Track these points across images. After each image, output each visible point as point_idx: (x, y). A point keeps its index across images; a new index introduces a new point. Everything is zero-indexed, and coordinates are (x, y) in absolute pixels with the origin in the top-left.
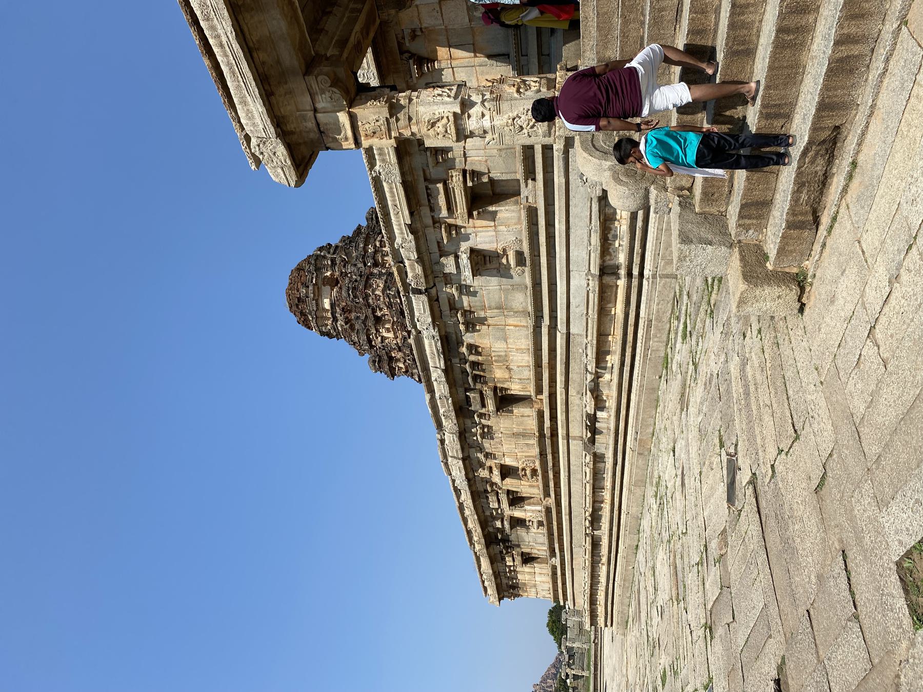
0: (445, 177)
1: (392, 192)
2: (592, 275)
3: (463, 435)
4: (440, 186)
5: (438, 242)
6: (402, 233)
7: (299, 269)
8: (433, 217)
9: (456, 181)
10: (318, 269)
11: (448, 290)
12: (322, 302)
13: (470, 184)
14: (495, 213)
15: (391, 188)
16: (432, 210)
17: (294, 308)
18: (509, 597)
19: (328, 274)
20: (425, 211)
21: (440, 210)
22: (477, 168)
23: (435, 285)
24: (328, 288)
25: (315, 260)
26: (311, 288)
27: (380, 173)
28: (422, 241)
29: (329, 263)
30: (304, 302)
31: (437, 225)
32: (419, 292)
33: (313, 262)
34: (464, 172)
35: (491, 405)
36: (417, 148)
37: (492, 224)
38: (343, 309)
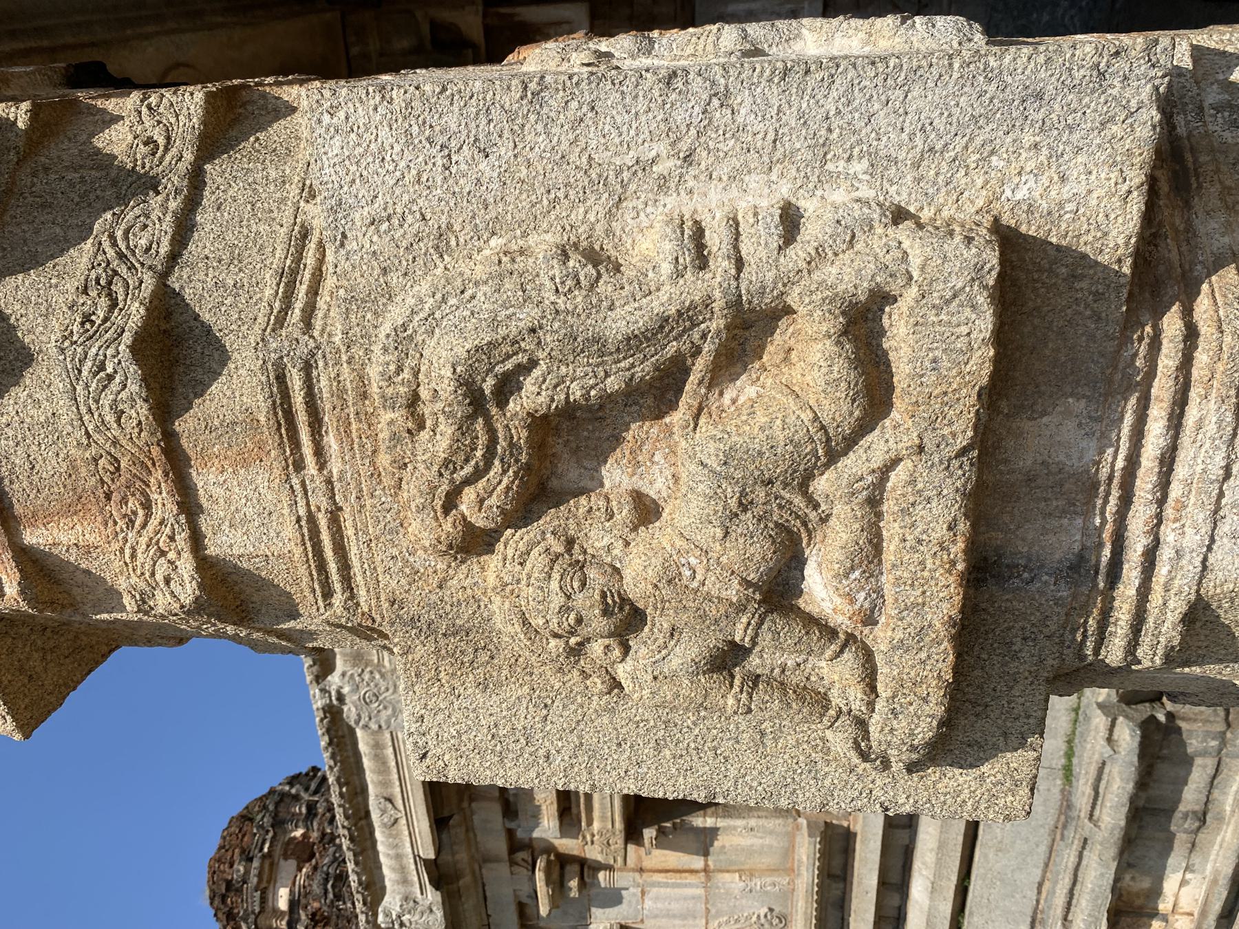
1: (379, 758)
5: (521, 907)
6: (405, 881)
7: (245, 818)
8: (510, 833)
10: (278, 823)
12: (275, 894)
14: (713, 832)
15: (377, 746)
17: (217, 901)
19: (298, 833)
21: (536, 815)
24: (292, 864)
25: (277, 804)
26: (256, 863)
27: (341, 698)
28: (469, 904)
29: (304, 810)
30: (239, 891)
31: (521, 855)
33: (271, 807)
37: (698, 862)
38: (314, 915)
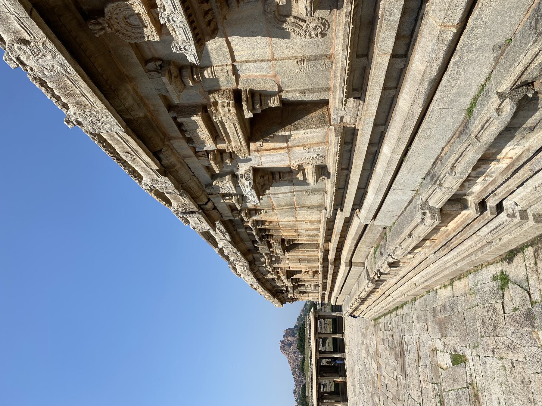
0: (203, 101)
2: (431, 209)
3: (254, 266)
4: (197, 119)
9: (225, 113)
11: (228, 201)
13: (248, 115)
16: (189, 141)
18: (290, 302)
20: (181, 145)
21: (203, 143)
22: (259, 86)
23: (209, 200)
32: (192, 213)
34: (237, 94)
35: (278, 251)
36: (141, 69)
37: (284, 145)
